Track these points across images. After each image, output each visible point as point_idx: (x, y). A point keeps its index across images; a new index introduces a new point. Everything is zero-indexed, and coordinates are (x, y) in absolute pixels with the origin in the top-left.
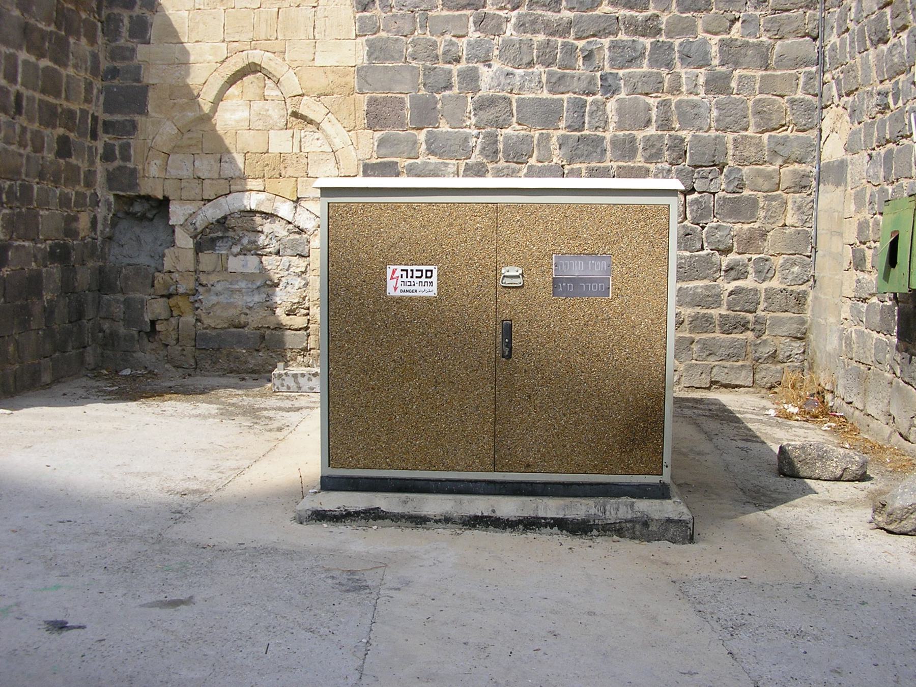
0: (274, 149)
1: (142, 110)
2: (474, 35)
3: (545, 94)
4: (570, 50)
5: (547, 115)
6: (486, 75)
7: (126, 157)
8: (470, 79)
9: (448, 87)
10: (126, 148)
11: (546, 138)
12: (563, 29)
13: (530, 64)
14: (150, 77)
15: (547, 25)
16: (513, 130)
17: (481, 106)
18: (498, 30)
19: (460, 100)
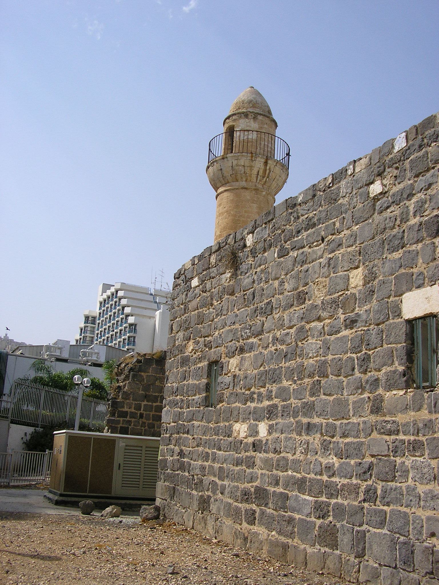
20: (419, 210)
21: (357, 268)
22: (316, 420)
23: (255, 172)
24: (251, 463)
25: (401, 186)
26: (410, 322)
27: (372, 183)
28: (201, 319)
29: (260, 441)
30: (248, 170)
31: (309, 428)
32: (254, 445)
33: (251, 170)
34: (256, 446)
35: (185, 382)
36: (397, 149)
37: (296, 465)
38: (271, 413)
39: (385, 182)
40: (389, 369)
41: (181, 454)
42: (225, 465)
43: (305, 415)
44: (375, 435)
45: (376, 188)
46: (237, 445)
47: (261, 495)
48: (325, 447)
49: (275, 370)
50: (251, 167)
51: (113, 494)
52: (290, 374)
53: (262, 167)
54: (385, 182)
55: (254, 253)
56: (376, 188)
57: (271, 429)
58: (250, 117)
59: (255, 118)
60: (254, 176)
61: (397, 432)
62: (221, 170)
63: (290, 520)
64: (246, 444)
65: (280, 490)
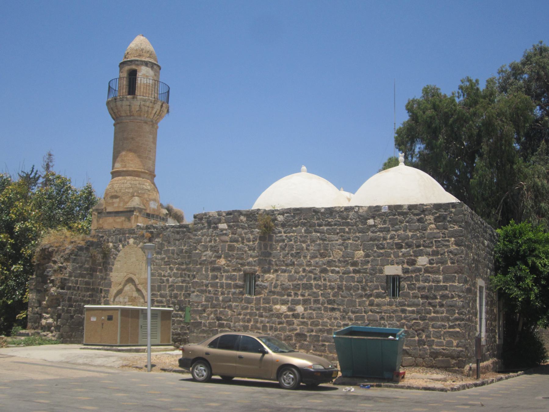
0: (134, 296)
1: (110, 287)
2: (169, 271)
3: (181, 284)
4: (185, 274)
5: (180, 288)
6: (171, 280)
7: (107, 297)
8: (168, 280)
9: (164, 282)
10: (107, 295)
11: (181, 294)
12: (184, 270)
13: (178, 277)
14: (112, 280)
15: (182, 268)
16: (175, 292)
17: (170, 286)
18: (172, 270)
19: (166, 286)
20: (392, 238)
21: (360, 250)
22: (336, 306)
23: (154, 112)
24: (290, 323)
25: (384, 226)
26: (387, 276)
27: (369, 219)
28: (231, 248)
29: (298, 314)
30: (150, 110)
31: (333, 310)
32: (293, 315)
33: (152, 110)
34: (296, 316)
35: (218, 280)
36: (383, 211)
37: (324, 324)
38: (305, 302)
39: (376, 221)
40: (377, 291)
41: (219, 319)
42: (268, 325)
43: (329, 304)
44: (370, 313)
45: (371, 222)
46: (279, 316)
47: (301, 336)
48: (343, 318)
49: (306, 284)
50: (153, 108)
51: (139, 344)
52: (318, 287)
53: (159, 109)
54: (376, 221)
55: (283, 225)
56: (371, 222)
57: (305, 309)
58: (149, 65)
59: (152, 68)
60: (153, 115)
61: (381, 312)
62: (129, 105)
63: (323, 345)
64: (287, 315)
65: (314, 334)
